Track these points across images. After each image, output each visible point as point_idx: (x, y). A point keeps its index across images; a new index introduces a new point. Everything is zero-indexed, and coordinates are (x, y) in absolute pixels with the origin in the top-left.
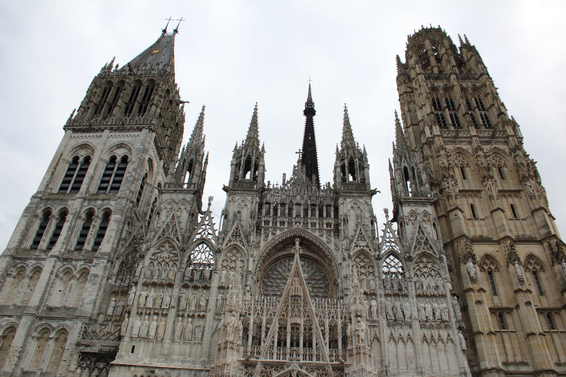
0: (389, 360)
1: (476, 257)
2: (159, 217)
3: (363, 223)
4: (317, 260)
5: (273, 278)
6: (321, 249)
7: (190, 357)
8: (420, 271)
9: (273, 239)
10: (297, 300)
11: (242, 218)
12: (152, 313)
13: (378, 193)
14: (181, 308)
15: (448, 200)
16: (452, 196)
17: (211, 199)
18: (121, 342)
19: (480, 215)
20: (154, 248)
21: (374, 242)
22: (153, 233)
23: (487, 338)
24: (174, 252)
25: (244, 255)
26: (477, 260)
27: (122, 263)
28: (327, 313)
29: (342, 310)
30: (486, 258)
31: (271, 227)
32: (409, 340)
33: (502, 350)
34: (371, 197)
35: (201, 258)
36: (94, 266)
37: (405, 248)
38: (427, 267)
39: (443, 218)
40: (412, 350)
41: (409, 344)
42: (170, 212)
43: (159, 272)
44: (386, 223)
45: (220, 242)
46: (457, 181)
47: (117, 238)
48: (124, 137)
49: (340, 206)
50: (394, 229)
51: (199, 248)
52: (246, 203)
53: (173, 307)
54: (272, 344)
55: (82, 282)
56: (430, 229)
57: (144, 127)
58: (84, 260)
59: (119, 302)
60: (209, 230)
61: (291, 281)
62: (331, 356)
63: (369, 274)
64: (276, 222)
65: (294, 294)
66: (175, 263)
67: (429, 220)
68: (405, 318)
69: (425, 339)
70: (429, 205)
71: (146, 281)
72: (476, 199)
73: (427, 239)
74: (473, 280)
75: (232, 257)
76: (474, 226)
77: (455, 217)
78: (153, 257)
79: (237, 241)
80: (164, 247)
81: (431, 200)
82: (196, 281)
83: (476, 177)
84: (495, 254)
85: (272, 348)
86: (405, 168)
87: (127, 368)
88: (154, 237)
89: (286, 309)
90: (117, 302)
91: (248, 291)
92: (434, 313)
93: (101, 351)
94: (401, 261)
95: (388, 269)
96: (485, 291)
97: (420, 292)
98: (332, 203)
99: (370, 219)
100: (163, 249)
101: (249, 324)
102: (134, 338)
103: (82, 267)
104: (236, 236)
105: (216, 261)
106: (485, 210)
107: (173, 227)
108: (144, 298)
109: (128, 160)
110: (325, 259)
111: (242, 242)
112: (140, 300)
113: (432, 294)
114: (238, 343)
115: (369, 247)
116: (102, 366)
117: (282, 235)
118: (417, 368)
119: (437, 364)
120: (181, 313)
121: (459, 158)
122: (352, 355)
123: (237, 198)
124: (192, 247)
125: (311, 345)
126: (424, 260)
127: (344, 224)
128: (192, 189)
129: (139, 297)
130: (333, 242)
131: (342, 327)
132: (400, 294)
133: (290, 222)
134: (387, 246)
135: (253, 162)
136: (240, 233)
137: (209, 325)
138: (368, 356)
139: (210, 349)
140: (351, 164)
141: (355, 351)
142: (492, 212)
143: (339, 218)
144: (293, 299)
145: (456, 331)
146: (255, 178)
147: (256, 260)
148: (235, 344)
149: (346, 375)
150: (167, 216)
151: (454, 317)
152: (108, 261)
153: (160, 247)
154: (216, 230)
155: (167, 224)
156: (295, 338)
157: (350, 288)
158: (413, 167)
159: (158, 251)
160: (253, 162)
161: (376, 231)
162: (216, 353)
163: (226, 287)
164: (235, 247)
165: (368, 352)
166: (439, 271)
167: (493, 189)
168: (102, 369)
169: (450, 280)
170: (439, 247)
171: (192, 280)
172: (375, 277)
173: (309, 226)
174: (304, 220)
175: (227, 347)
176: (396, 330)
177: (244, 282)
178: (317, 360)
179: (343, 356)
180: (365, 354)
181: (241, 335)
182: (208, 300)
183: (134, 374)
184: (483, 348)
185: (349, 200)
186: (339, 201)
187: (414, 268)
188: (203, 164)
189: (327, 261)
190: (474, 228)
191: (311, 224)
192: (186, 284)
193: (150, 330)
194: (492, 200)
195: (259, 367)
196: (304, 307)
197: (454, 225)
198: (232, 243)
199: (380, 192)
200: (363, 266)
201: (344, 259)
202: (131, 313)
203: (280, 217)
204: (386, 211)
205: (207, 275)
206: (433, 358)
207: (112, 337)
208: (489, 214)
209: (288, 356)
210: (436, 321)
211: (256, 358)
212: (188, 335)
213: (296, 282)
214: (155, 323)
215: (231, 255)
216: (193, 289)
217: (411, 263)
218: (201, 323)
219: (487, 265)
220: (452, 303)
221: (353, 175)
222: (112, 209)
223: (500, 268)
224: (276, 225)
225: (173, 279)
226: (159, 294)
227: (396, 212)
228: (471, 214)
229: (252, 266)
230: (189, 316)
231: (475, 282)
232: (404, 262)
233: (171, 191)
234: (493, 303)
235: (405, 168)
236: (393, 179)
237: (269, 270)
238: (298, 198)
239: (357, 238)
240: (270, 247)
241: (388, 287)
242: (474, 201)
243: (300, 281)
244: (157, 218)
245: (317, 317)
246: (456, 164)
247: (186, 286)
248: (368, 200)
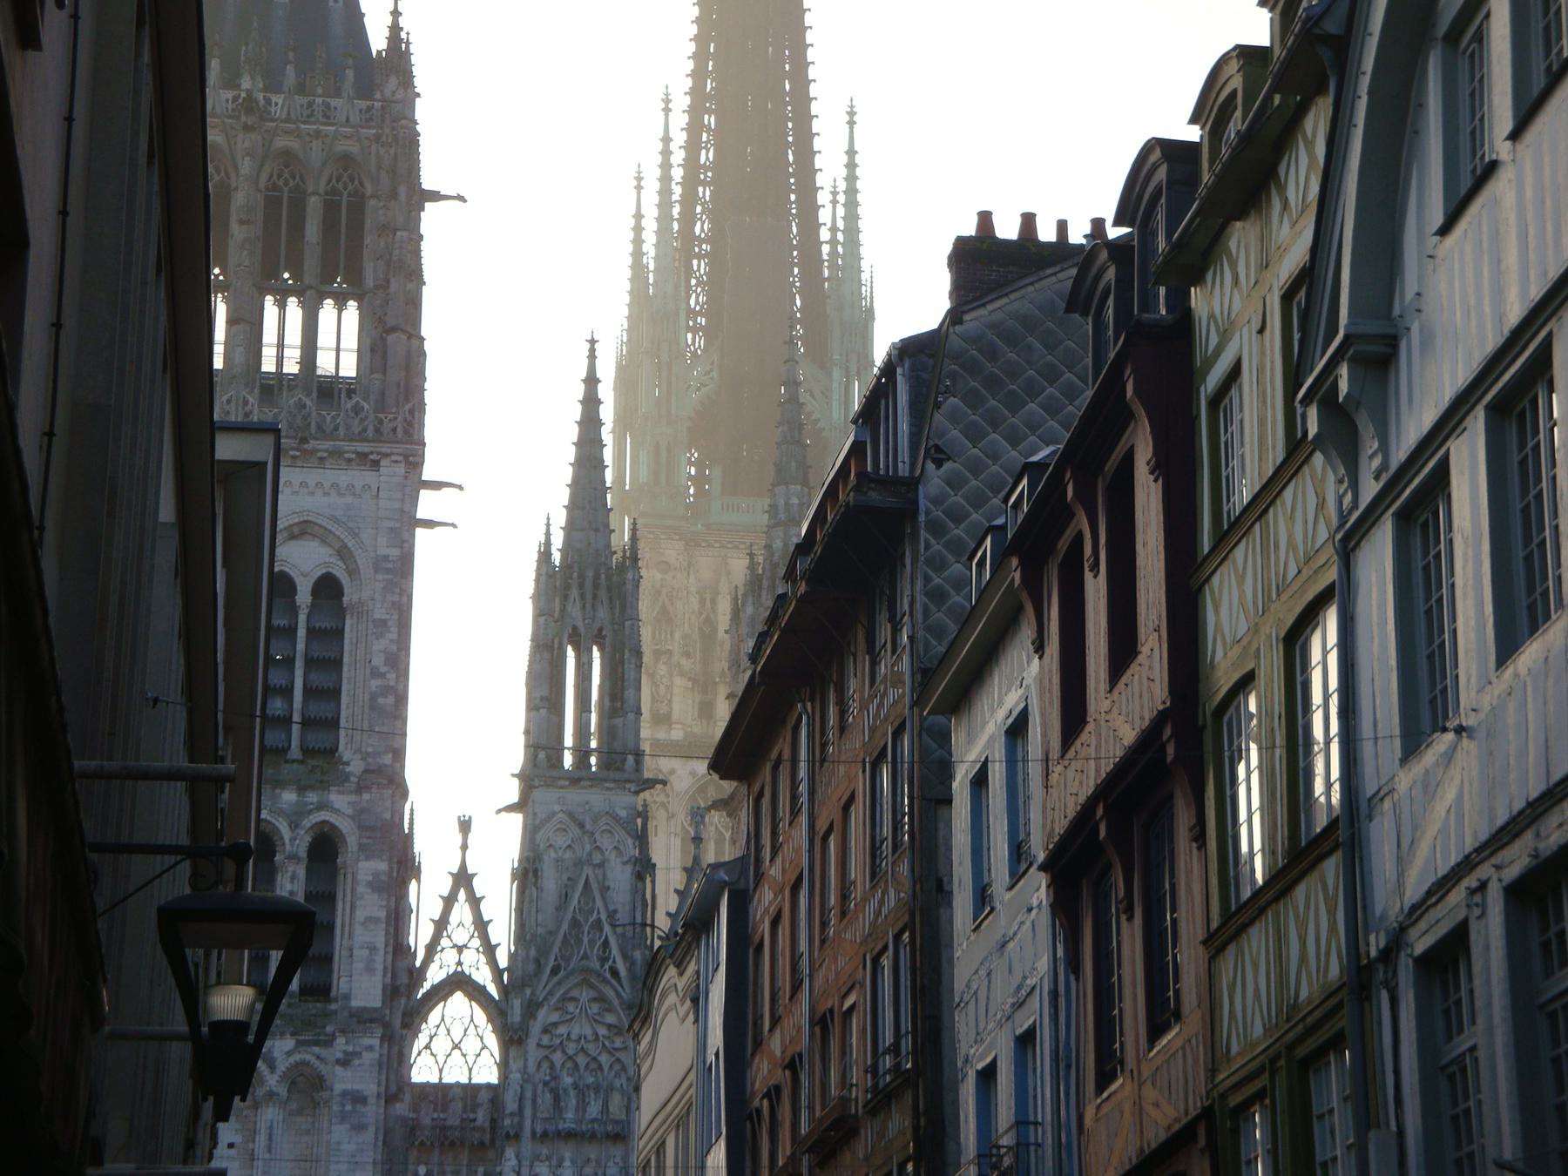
24: (610, 1019)
36: (345, 1062)
43: (577, 1096)
47: (390, 949)
48: (312, 494)
55: (300, 1112)
57: (386, 455)
58: (293, 1034)
66: (618, 1060)
78: (546, 1040)
80: (573, 999)
100: (571, 1007)
103: (292, 1060)
152: (382, 1039)
155: (573, 918)
159: (555, 1017)
222: (345, 826)
225: (624, 1117)
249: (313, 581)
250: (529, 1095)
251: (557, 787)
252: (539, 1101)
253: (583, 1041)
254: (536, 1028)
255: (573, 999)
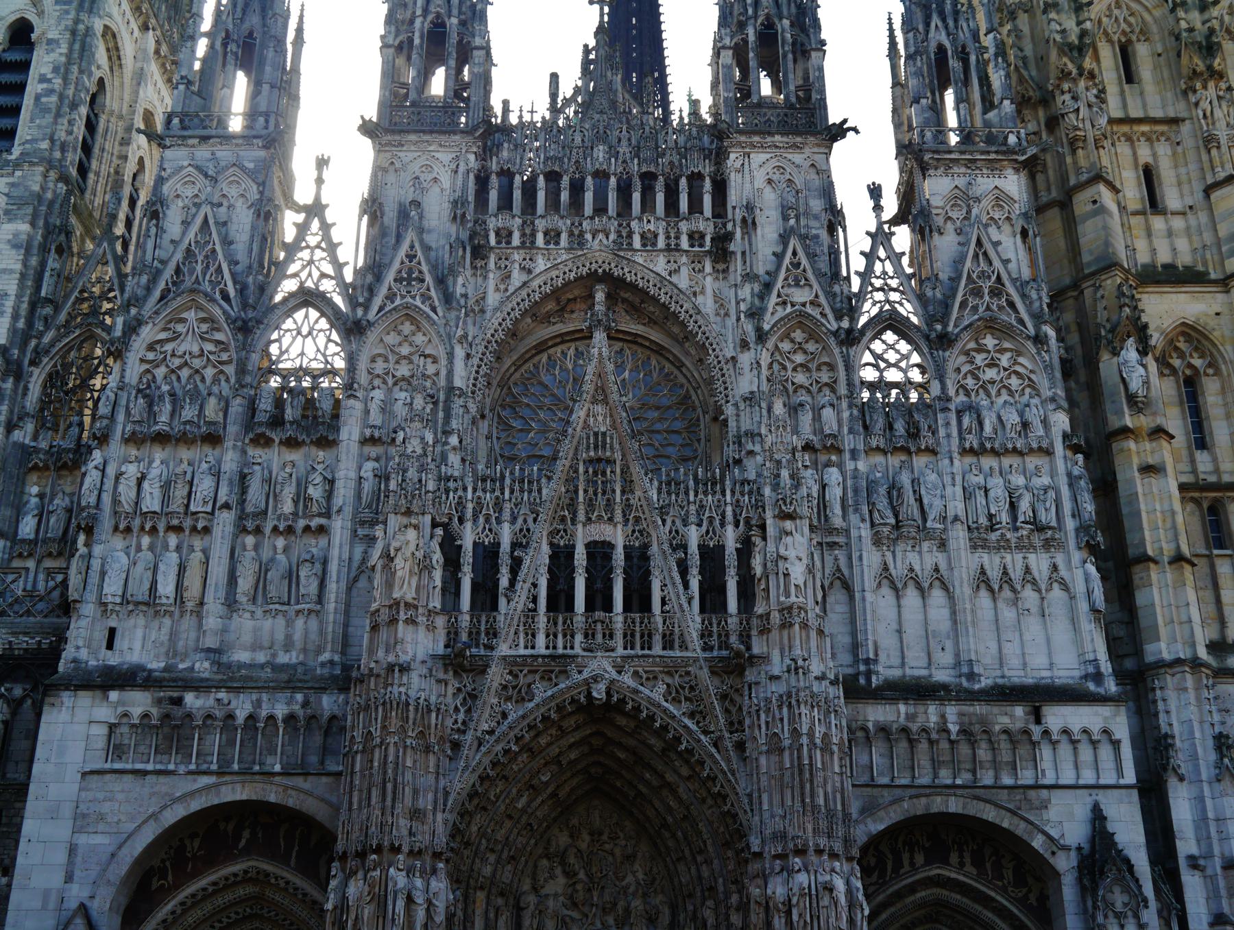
0: (875, 643)
1: (1150, 332)
2: (157, 226)
3: (803, 231)
4: (663, 348)
5: (528, 405)
6: (675, 315)
7: (287, 651)
8: (977, 378)
9: (525, 284)
10: (604, 473)
11: (426, 223)
12: (161, 527)
13: (851, 134)
14: (249, 509)
15: (1074, 152)
16: (1085, 141)
17: (322, 163)
18: (73, 620)
19: (1172, 198)
20: (150, 325)
21: (837, 288)
22: (144, 279)
23: (1169, 575)
25: (436, 340)
26: (1153, 342)
27: (50, 375)
28: (693, 508)
29: (738, 501)
30: (1183, 333)
31: (518, 248)
32: (937, 583)
33: (1211, 609)
34: (830, 148)
35: (302, 354)
37: (931, 308)
38: (997, 365)
39: (1054, 214)
40: (945, 612)
41: (937, 595)
42: (194, 210)
44: (873, 230)
45: (361, 300)
46: (1103, 91)
47: (26, 299)
49: (733, 175)
50: (898, 250)
51: (295, 322)
52: (435, 175)
53: (226, 506)
54: (531, 606)
56: (1012, 248)
59: (51, 500)
60: (323, 262)
61: (582, 414)
62: (705, 634)
63: (820, 390)
64: (533, 235)
65: (592, 454)
66: (222, 372)
67: (1008, 218)
68: (925, 520)
69: (982, 579)
70: (1010, 171)
71: (134, 433)
72: (1163, 149)
73: (999, 278)
74: (1136, 403)
75: (400, 344)
76: (1149, 234)
77: (1090, 207)
78: (151, 356)
79: (414, 297)
80: (183, 321)
81: (1016, 153)
82: (292, 423)
83: (1166, 74)
84: (1212, 323)
85: (533, 618)
86: (941, 49)
87: (98, 693)
88: (149, 289)
89: (572, 499)
90: (46, 500)
91: (454, 449)
92: (1013, 507)
93: (11, 649)
94: (917, 348)
95: (877, 374)
96: (1172, 437)
97: (972, 441)
98: (707, 169)
99: (825, 218)
100: (180, 328)
101: (460, 547)
102: (110, 607)
104: (409, 280)
105: (351, 360)
106: (1190, 181)
107: (207, 257)
108: (133, 483)
109: (34, 36)
110: (687, 345)
111: (430, 298)
112: (121, 488)
113: (1010, 446)
114: (431, 605)
115: (819, 306)
116: (18, 691)
117: (554, 273)
118: (957, 664)
119: (1018, 651)
120: (250, 525)
121: (1116, 12)
122: (769, 631)
123: (406, 155)
124: (274, 317)
125: (646, 606)
126: (990, 342)
127: (743, 234)
128: (264, 132)
129: (117, 478)
130: (709, 291)
131: (737, 549)
132: (913, 449)
133: (576, 232)
134: (874, 304)
135: (453, 39)
136: (420, 272)
137: (340, 558)
138: (813, 634)
139: (346, 625)
140: (768, 36)
141: (776, 618)
142: (1208, 191)
143: (730, 216)
144: (591, 470)
145: (1077, 556)
146: (457, 88)
147: (473, 353)
148: (420, 610)
149: (750, 689)
150: (186, 224)
151: (1073, 516)
153: (170, 322)
154: (347, 263)
155: (188, 251)
156: (599, 585)
157: (764, 431)
158: (964, 47)
159: (163, 336)
160: (453, 39)
161: (843, 257)
162: (366, 636)
163: (384, 439)
164: (410, 315)
165: (813, 622)
166: (1033, 376)
167: (1218, 113)
168: (19, 702)
169: (1066, 405)
170: (1037, 304)
171: (277, 421)
172: (839, 398)
173: (637, 242)
174: (620, 225)
175: (397, 620)
176: (899, 555)
177: (440, 421)
178: (664, 648)
179: (741, 635)
180: (805, 626)
181: (438, 583)
182: (332, 482)
183: (120, 710)
184: (1153, 605)
185: (758, 158)
186: (729, 163)
187: (958, 370)
188: (290, 48)
189: (693, 352)
190: (1151, 242)
191: (643, 236)
192: (263, 435)
193: (160, 578)
194: (1214, 152)
195: (496, 675)
196: (623, 492)
197: (1088, 233)
198: (398, 302)
199: (857, 132)
200: (801, 365)
201: (744, 345)
202: (95, 530)
203: (542, 217)
204: (875, 192)
205: (327, 405)
206: (1007, 635)
207: (41, 606)
208: (1200, 195)
209: (579, 638)
210: (1016, 529)
211: (487, 647)
212: (276, 587)
213: (600, 418)
214: (173, 557)
215: (398, 339)
216: (283, 449)
217: (947, 353)
218: (314, 550)
219: (1182, 355)
220: (1069, 475)
221: (773, 75)
223: (1223, 367)
224: (533, 242)
225: (220, 418)
226: (179, 470)
227: (908, 194)
228: (1142, 199)
229: (464, 374)
230: (275, 529)
231: (1140, 411)
232: (926, 350)
233: (191, 142)
234: (1194, 471)
235: (941, 49)
236: (902, 86)
237: (515, 384)
238: (600, 152)
239: (786, 279)
240: (517, 313)
241: (880, 423)
242: (1154, 155)
243: (611, 416)
244: (153, 230)
245: (664, 521)
246: (1106, 33)
247: (262, 441)
248: (819, 158)
249: (7, 24)
250: (124, 402)
251: (187, 146)
252: (132, 405)
253: (187, 356)
254: (138, 345)
255: (183, 321)
